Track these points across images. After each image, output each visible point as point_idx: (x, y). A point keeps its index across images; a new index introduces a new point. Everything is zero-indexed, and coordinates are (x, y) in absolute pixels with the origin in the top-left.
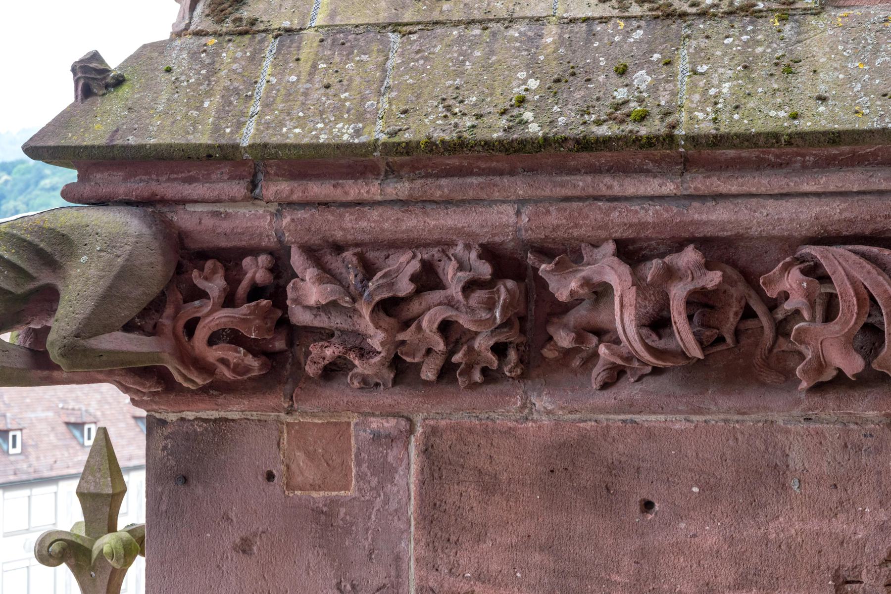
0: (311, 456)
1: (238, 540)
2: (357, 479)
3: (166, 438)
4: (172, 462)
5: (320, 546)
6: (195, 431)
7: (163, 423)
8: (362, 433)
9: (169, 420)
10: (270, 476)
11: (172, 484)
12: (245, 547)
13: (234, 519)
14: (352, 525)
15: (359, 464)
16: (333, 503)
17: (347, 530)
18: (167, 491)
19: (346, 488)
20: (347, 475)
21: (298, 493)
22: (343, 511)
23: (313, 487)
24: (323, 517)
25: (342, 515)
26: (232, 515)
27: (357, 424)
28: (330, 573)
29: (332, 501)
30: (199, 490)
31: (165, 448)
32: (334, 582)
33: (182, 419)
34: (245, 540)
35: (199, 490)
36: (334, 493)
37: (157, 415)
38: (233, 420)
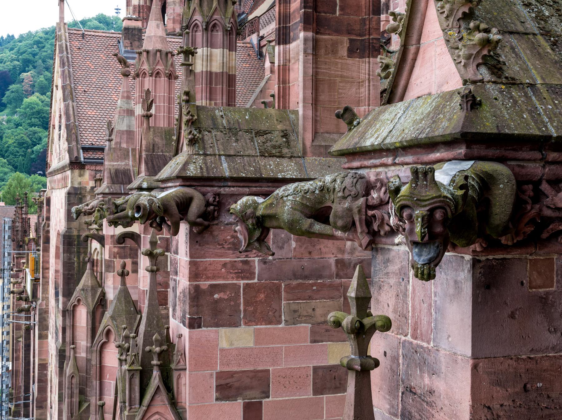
0: (539, 273)
1: (510, 313)
2: (557, 283)
3: (481, 268)
4: (483, 279)
5: (542, 313)
6: (493, 264)
7: (479, 261)
8: (558, 262)
9: (482, 260)
10: (522, 283)
11: (483, 289)
12: (512, 316)
13: (509, 304)
14: (554, 302)
15: (557, 276)
16: (547, 293)
17: (553, 305)
18: (481, 292)
19: (552, 287)
20: (553, 281)
21: (534, 290)
22: (551, 297)
23: (540, 287)
24: (543, 300)
25: (551, 298)
26: (508, 301)
27: (556, 259)
28: (546, 324)
29: (547, 293)
30: (494, 291)
31: (480, 273)
32: (548, 328)
33: (488, 259)
34: (512, 312)
35: (494, 291)
36: (548, 289)
37: (477, 258)
38: (508, 259)
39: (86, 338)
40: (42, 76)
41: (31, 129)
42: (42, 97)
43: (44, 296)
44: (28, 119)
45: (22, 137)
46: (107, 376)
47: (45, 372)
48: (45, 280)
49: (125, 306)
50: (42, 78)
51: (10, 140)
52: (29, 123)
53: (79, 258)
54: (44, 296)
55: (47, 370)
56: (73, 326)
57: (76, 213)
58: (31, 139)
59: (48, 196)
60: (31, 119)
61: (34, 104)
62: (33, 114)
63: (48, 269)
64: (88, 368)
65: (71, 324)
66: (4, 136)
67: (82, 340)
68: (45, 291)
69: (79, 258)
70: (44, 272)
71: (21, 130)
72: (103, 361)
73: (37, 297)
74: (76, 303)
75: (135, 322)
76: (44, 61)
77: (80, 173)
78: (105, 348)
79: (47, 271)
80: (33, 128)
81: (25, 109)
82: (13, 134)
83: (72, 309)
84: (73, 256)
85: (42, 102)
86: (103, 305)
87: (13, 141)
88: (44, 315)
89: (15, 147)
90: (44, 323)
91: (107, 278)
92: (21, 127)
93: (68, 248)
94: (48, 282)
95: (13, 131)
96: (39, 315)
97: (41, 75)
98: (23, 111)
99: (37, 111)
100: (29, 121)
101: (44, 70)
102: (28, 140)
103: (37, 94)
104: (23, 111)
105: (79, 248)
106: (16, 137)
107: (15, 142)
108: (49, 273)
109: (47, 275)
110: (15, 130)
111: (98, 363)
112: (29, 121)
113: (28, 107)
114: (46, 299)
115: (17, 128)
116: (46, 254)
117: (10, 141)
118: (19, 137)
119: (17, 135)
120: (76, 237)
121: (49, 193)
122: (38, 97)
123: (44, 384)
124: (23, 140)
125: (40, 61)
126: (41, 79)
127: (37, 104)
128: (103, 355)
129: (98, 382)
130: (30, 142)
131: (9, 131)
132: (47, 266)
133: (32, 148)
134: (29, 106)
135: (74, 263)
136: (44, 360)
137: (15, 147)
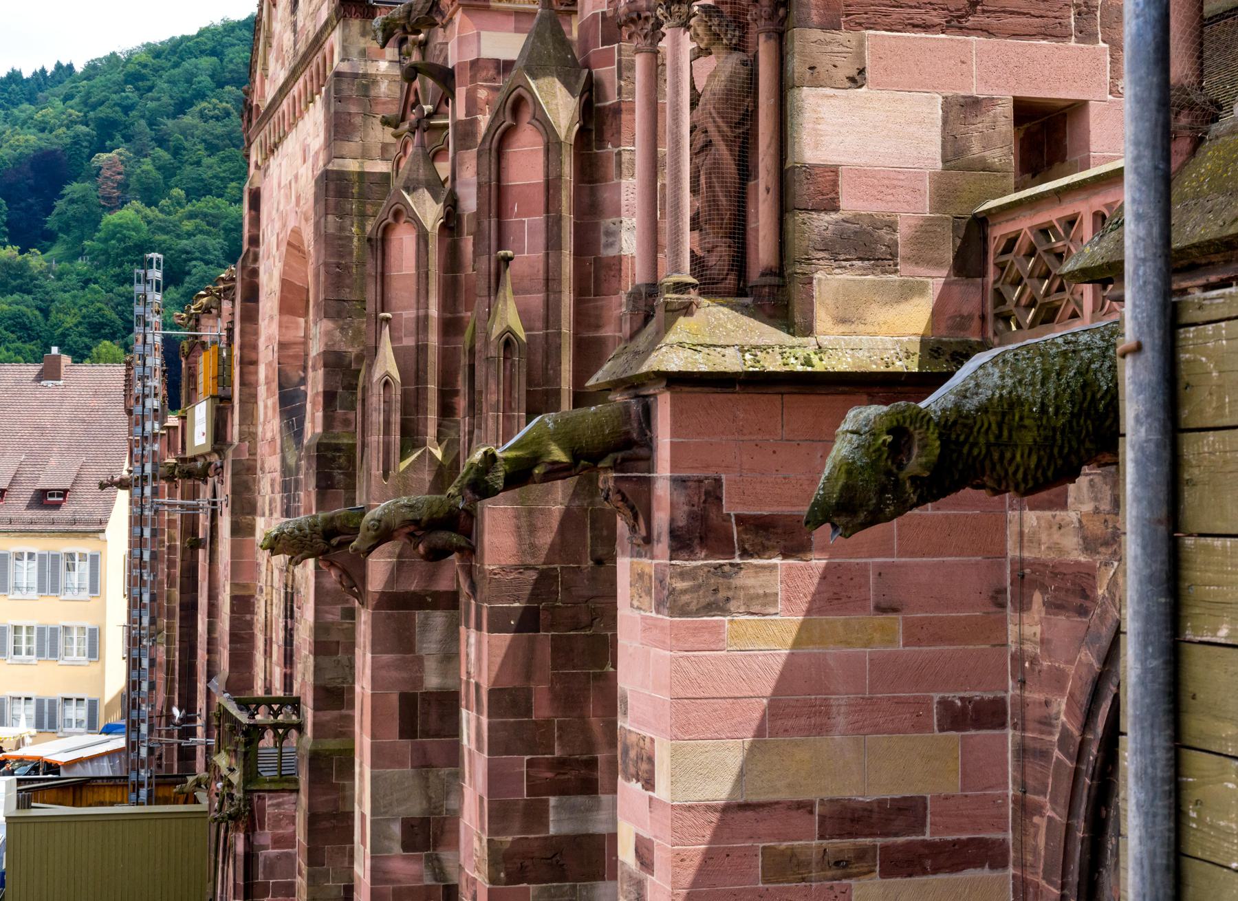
39: (413, 301)
40: (148, 160)
41: (122, 289)
42: (148, 211)
43: (245, 428)
44: (114, 266)
45: (100, 309)
46: (513, 209)
47: (248, 617)
48: (246, 390)
49: (555, 49)
50: (147, 165)
51: (68, 319)
52: (117, 275)
53: (362, 227)
54: (245, 428)
55: (252, 612)
56: (383, 274)
57: (384, 31)
58: (121, 314)
59: (254, 186)
60: (120, 266)
61: (128, 229)
62: (126, 251)
63: (255, 363)
64: (421, 367)
65: (379, 270)
66: (53, 308)
67: (404, 309)
68: (249, 416)
69: (362, 227)
70: (245, 370)
71: (96, 292)
72: (503, 177)
73: (225, 439)
74: (390, 220)
75: (577, 82)
76: (152, 123)
77: (364, 27)
78: (509, 147)
79: (252, 368)
80: (127, 286)
81: (106, 240)
82: (75, 304)
83: (380, 235)
84: (348, 222)
85: (149, 223)
86: (452, 229)
87: (75, 321)
88: (245, 477)
89: (81, 335)
90: (246, 496)
91: (461, 165)
92: (96, 286)
93: (337, 204)
94: (255, 396)
95: (75, 297)
96: (233, 475)
97: (146, 156)
98: (101, 246)
99: (136, 245)
100: (117, 270)
101: (153, 144)
102: (114, 316)
103: (137, 204)
104: (101, 246)
105: (364, 204)
106: (84, 310)
107: (80, 323)
108: (256, 373)
109: (252, 378)
110: (81, 293)
111: (493, 177)
112: (117, 270)
113: (113, 238)
114: (249, 436)
115: (83, 288)
116: (248, 326)
117: (70, 321)
118: (92, 309)
119: (86, 306)
120: (356, 177)
121: (256, 180)
122: (137, 211)
123: (244, 646)
124: (103, 316)
125: (143, 122)
126: (144, 167)
127: (137, 229)
128: (504, 164)
129: (493, 221)
130: (119, 322)
131: (67, 295)
132: (253, 356)
133: (123, 337)
134: (116, 233)
135: (350, 239)
136: (245, 587)
137: (81, 335)
